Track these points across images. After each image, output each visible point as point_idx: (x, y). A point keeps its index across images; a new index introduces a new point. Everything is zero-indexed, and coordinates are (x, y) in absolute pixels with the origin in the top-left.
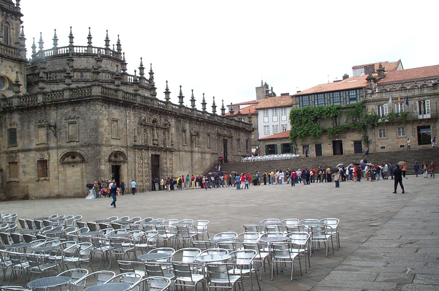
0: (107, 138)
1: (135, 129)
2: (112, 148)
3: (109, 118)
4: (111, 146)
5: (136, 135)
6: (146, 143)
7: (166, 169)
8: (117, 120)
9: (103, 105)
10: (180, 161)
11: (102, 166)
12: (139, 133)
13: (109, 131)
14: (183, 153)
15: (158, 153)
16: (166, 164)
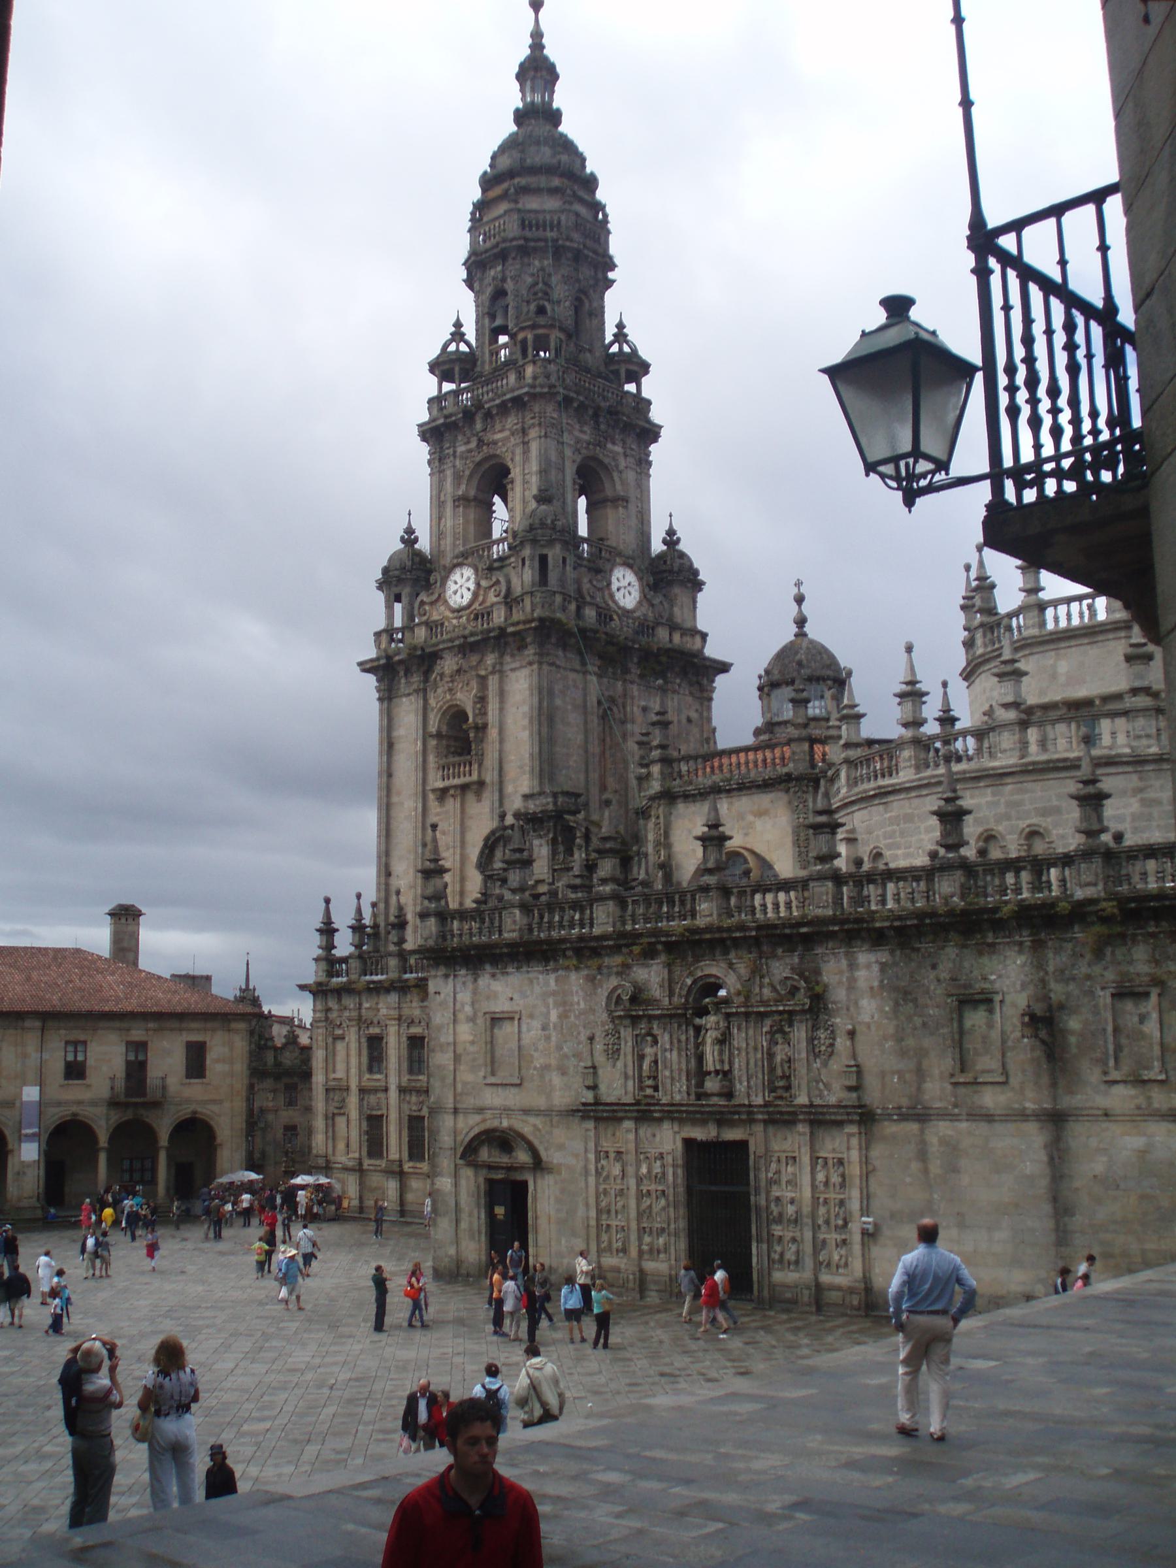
0: (465, 1084)
1: (591, 1039)
2: (484, 1121)
3: (475, 1014)
4: (480, 1110)
5: (600, 1058)
6: (649, 1091)
7: (791, 1210)
8: (511, 1015)
9: (446, 976)
10: (926, 1171)
11: (439, 1178)
12: (614, 1053)
13: (474, 1060)
14: (964, 1125)
15: (732, 1134)
16: (793, 1183)
